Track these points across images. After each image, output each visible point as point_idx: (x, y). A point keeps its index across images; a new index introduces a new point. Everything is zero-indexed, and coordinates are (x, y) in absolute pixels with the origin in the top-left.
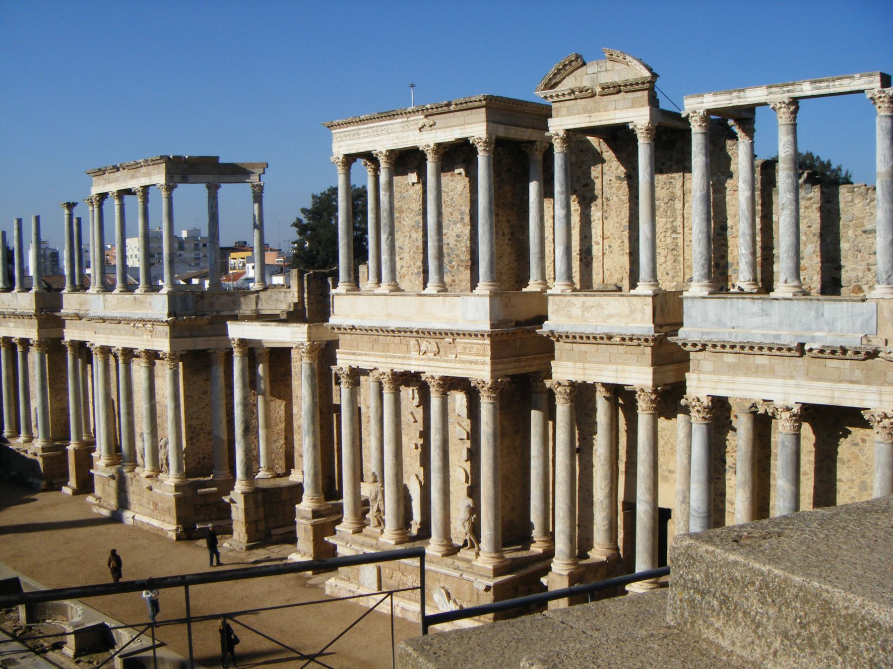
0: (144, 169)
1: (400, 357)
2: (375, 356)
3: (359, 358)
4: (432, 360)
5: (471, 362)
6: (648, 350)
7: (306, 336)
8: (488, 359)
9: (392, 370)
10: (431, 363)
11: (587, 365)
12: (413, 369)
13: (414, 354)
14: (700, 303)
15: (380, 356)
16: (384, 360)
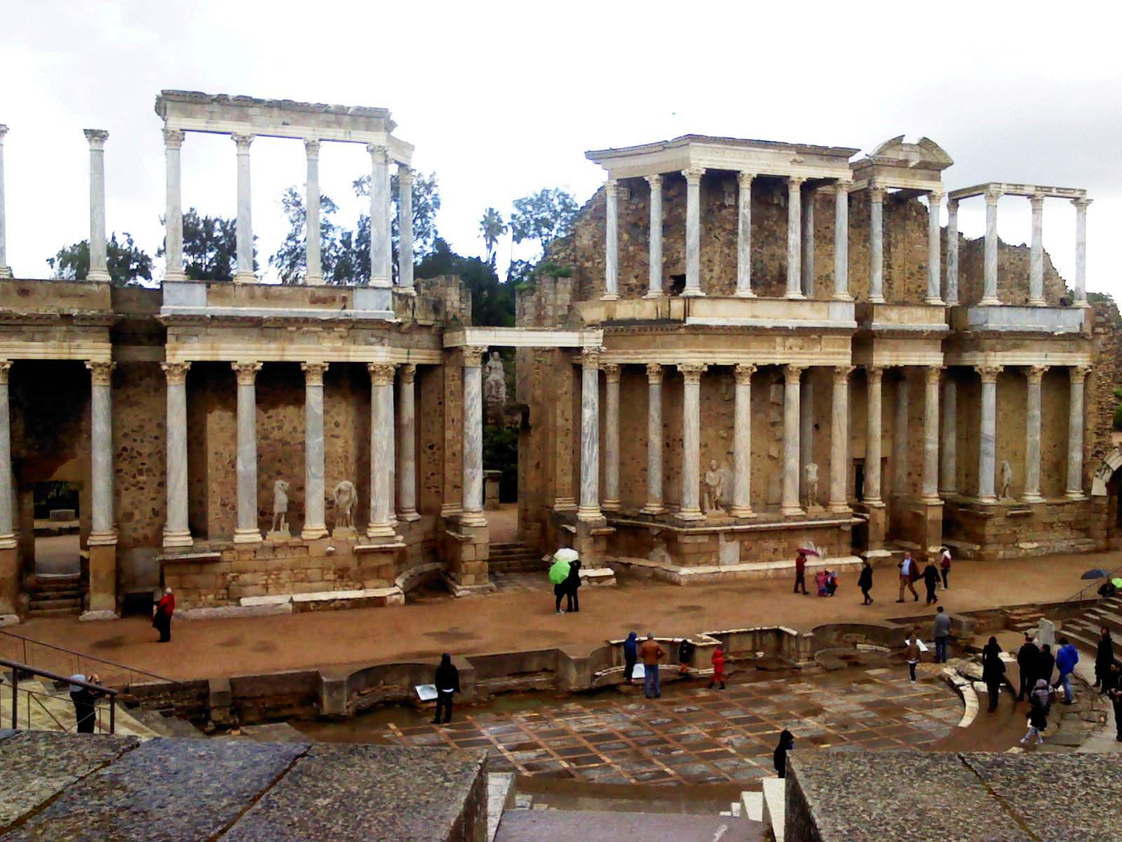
0: (332, 117)
1: (764, 353)
2: (736, 353)
3: (717, 355)
4: (799, 353)
5: (833, 353)
6: (940, 342)
7: (601, 341)
8: (849, 350)
9: (755, 364)
10: (796, 356)
11: (900, 353)
12: (777, 362)
13: (779, 349)
14: (997, 309)
15: (742, 353)
16: (747, 356)
